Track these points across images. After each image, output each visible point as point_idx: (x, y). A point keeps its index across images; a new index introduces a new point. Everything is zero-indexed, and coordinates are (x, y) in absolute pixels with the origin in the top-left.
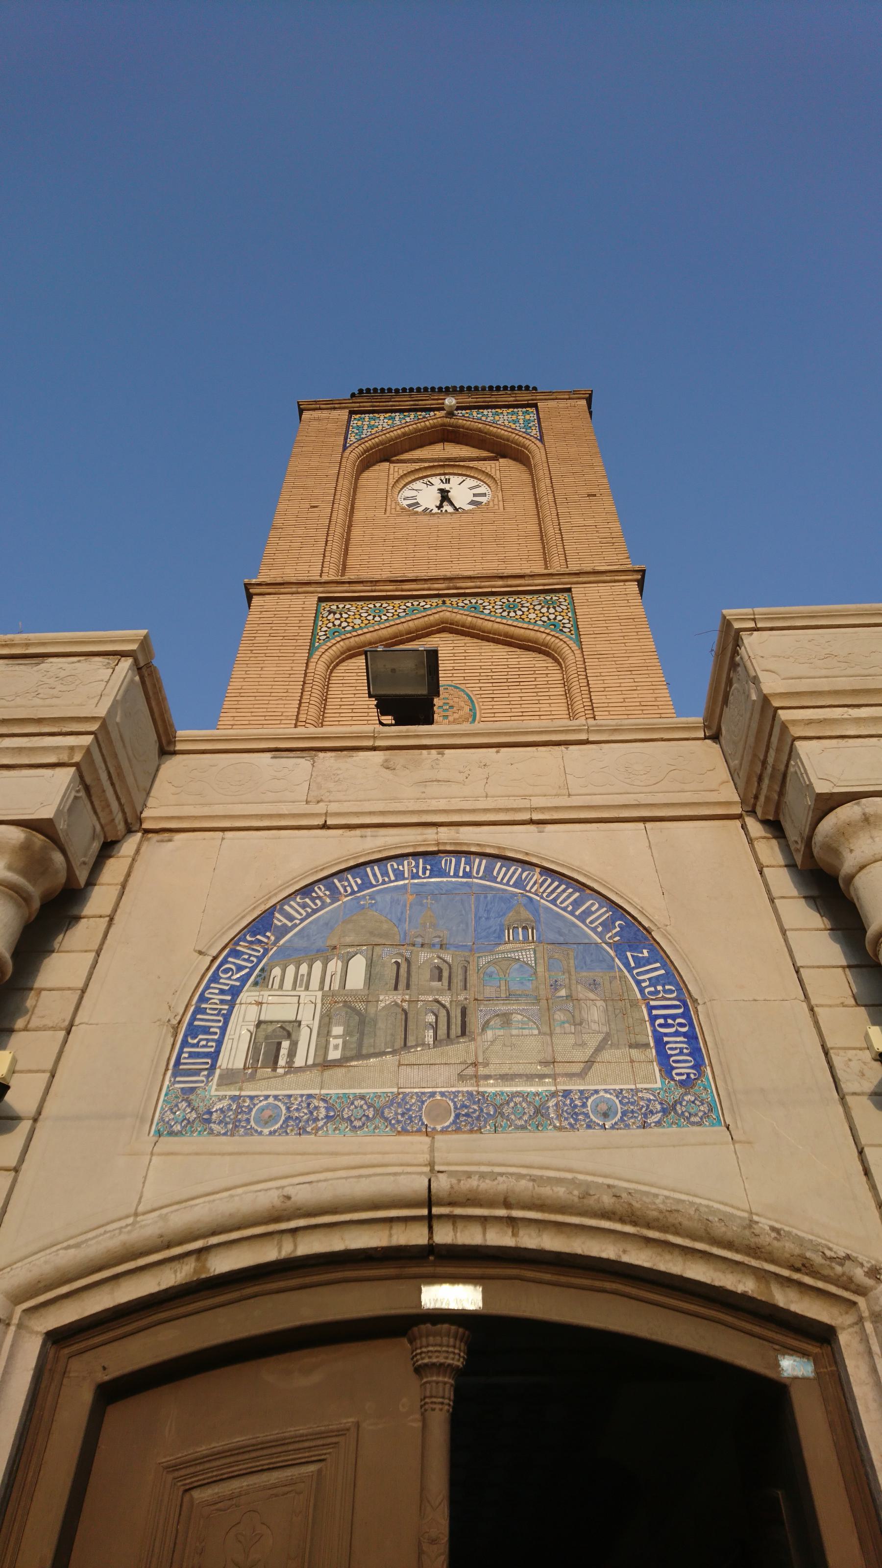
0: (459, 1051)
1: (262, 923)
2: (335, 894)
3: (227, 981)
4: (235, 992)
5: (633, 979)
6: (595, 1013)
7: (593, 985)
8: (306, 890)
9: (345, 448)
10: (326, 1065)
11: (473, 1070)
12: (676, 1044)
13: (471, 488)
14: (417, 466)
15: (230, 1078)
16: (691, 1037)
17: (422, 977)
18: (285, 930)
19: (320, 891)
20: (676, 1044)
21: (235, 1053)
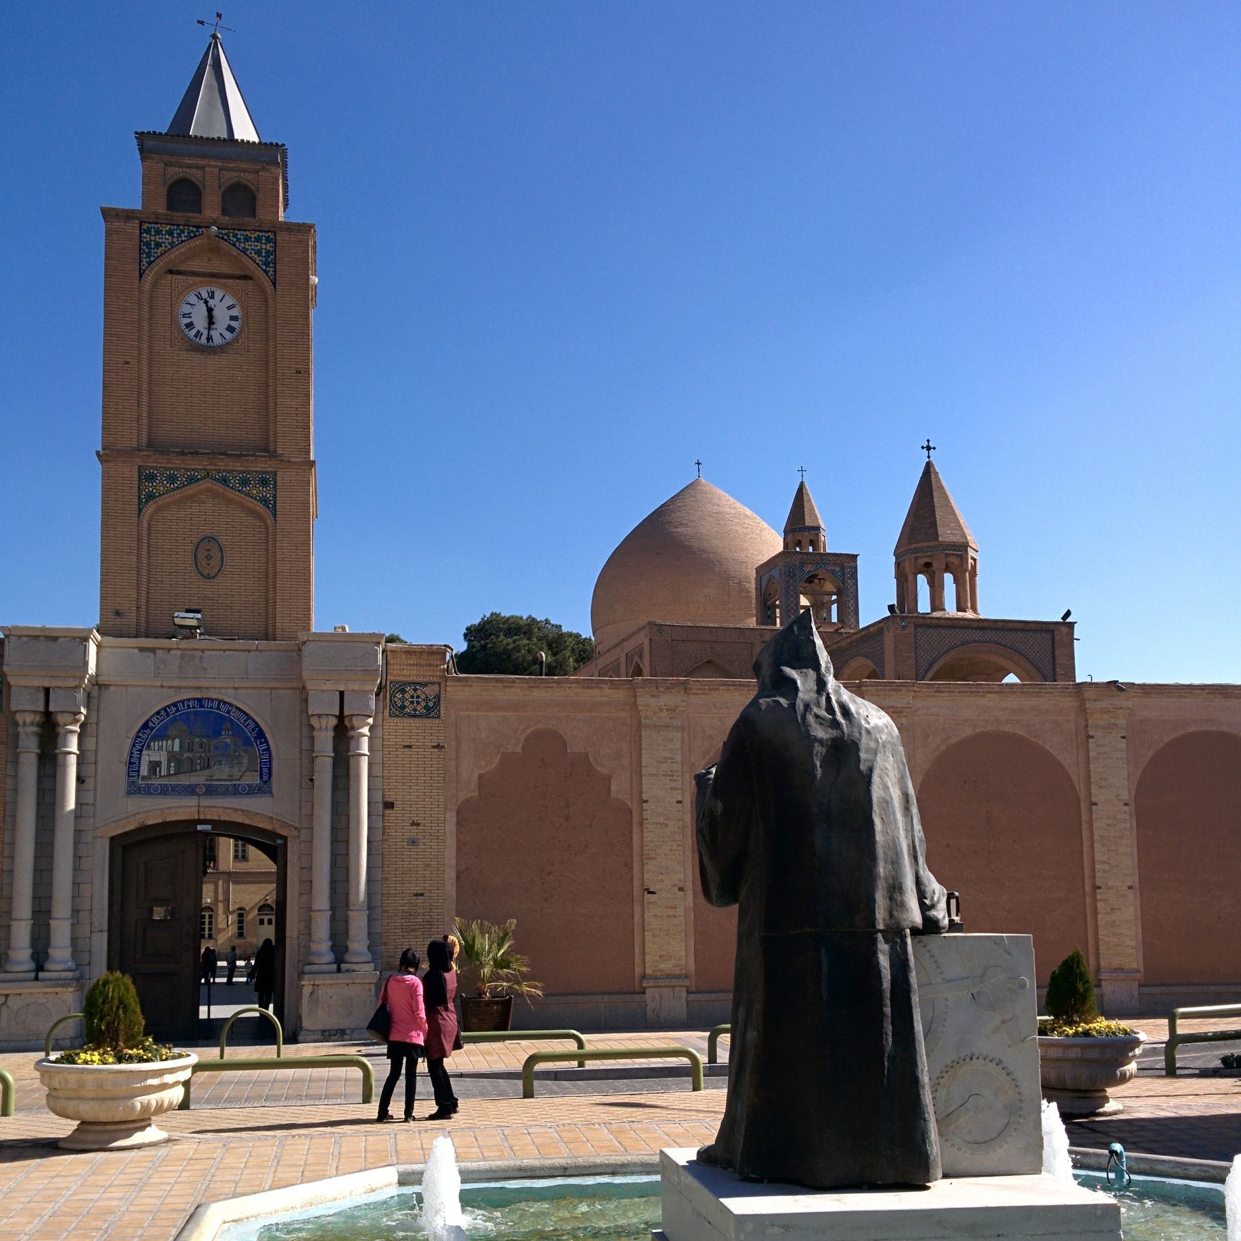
0: (206, 772)
1: (145, 726)
2: (168, 715)
3: (138, 747)
4: (141, 751)
5: (258, 749)
6: (245, 761)
7: (246, 751)
8: (158, 713)
9: (141, 276)
10: (169, 775)
11: (210, 778)
12: (265, 770)
13: (229, 308)
14: (191, 279)
15: (144, 778)
16: (270, 769)
17: (196, 747)
18: (152, 729)
19: (162, 713)
20: (265, 770)
21: (144, 771)
